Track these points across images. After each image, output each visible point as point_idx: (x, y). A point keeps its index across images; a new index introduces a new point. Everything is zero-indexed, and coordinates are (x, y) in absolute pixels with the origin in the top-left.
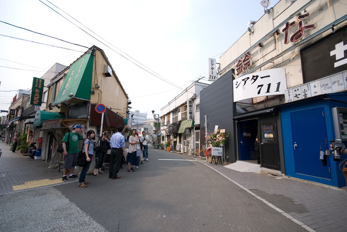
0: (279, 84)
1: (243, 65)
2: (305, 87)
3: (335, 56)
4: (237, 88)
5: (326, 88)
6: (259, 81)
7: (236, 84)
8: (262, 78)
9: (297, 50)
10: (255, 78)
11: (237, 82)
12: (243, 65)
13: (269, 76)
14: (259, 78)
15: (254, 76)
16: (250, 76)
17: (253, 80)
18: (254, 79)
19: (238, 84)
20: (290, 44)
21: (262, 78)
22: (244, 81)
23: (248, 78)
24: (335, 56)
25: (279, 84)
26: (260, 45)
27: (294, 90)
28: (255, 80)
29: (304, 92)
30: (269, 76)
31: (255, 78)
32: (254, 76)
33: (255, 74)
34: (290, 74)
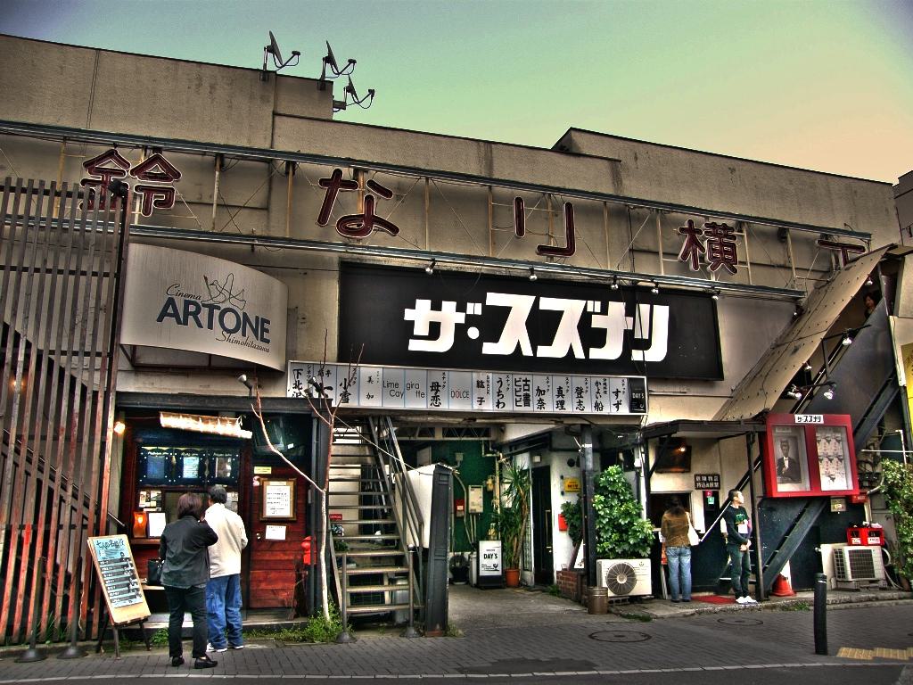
3: (412, 323)
5: (393, 393)
24: (412, 323)
29: (343, 385)
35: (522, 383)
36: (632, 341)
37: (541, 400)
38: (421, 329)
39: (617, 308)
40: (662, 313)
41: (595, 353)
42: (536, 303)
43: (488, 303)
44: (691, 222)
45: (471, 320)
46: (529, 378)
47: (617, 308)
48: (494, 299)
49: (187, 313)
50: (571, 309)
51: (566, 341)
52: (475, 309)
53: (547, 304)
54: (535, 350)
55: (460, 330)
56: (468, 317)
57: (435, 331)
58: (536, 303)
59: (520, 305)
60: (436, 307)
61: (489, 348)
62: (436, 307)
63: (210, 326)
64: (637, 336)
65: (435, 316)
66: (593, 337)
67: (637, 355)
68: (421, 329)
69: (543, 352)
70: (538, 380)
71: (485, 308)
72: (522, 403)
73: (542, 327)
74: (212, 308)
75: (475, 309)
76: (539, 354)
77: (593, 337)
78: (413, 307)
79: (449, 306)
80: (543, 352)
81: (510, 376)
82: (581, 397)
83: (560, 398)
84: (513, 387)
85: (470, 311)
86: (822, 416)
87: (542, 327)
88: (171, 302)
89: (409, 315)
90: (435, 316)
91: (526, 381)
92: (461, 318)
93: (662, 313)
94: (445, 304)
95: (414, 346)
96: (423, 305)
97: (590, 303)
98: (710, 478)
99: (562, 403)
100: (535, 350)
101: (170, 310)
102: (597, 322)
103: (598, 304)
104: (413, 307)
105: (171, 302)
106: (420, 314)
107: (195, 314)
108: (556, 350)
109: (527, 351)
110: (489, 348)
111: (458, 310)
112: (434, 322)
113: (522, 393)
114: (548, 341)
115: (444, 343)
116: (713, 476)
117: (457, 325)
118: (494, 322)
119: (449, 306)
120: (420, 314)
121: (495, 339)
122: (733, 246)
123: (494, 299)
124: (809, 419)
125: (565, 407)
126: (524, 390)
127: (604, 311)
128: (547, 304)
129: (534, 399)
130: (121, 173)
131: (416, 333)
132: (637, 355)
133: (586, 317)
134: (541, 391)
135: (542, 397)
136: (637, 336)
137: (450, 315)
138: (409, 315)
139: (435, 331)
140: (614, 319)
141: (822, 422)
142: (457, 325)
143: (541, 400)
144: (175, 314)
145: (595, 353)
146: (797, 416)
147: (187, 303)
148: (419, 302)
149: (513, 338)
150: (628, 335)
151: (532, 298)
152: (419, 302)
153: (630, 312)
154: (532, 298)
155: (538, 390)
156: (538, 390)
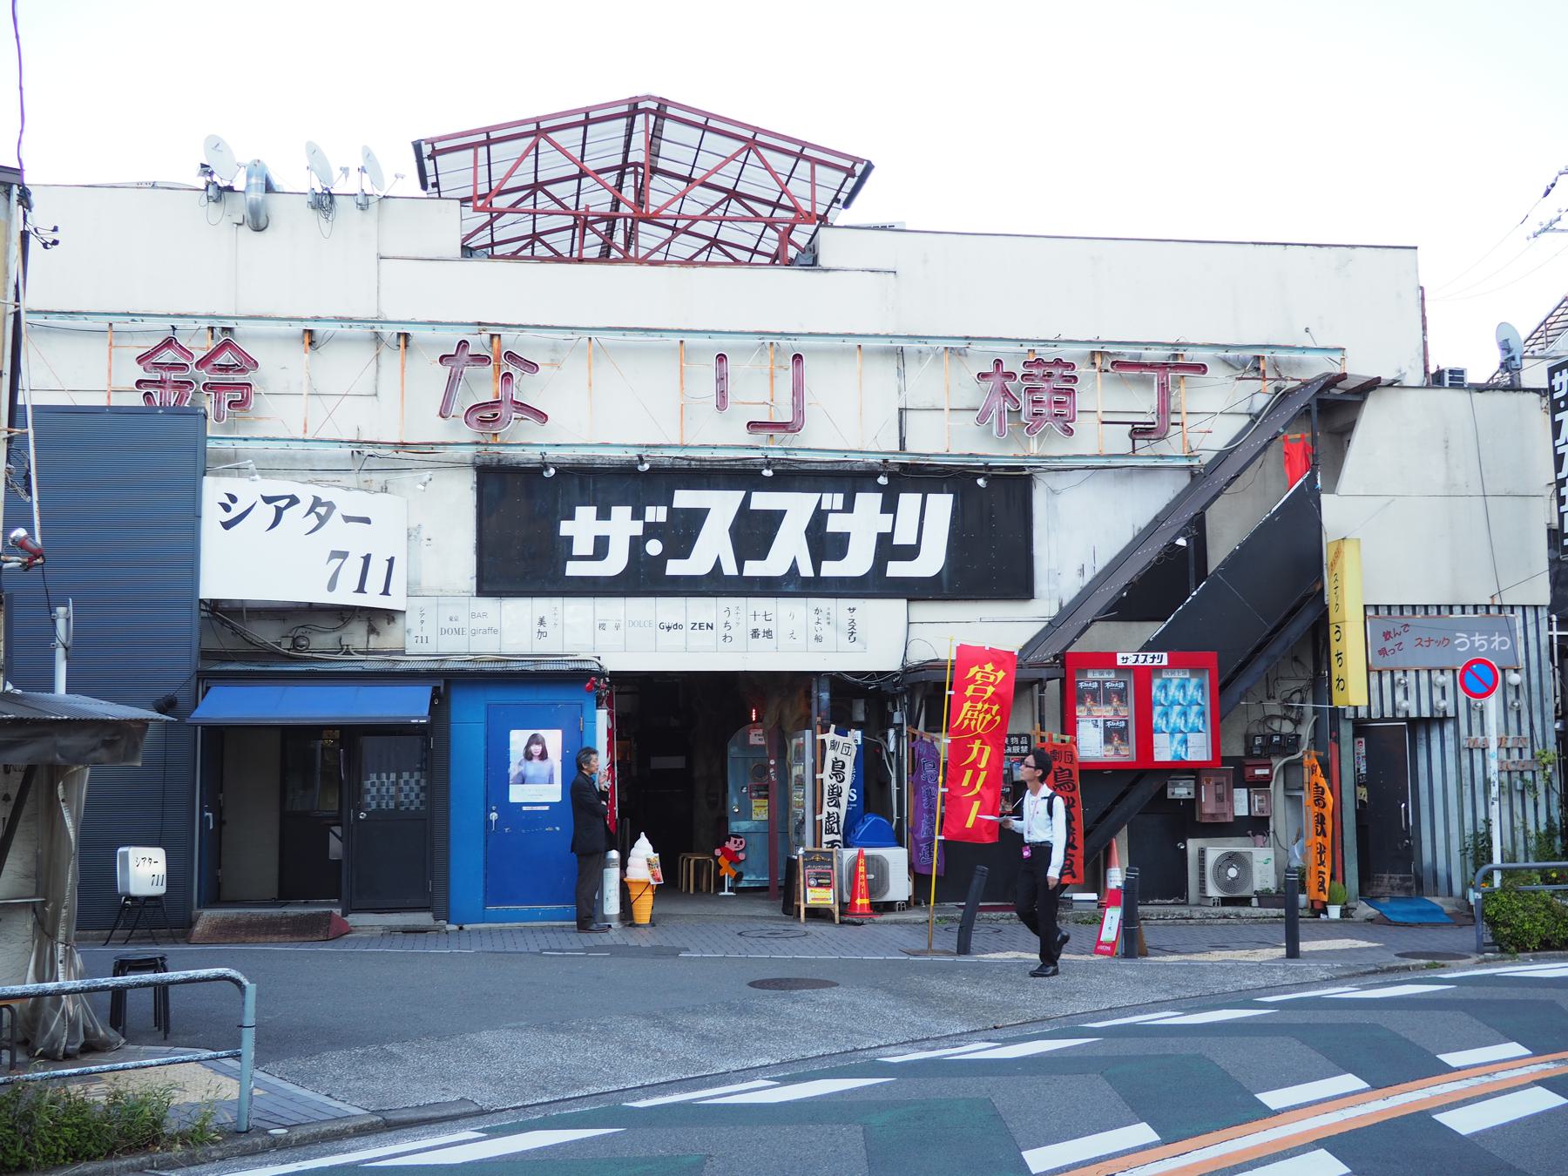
0: (391, 561)
3: (570, 540)
4: (227, 525)
6: (337, 533)
7: (227, 508)
8: (348, 519)
10: (321, 510)
11: (233, 499)
13: (367, 521)
14: (336, 517)
15: (317, 502)
16: (306, 494)
17: (313, 520)
18: (318, 514)
19: (237, 509)
20: (468, 434)
21: (348, 519)
22: (270, 510)
23: (294, 500)
24: (570, 540)
25: (391, 561)
28: (322, 520)
30: (367, 521)
31: (322, 510)
32: (317, 502)
33: (326, 495)
34: (424, 535)
36: (887, 548)
38: (583, 546)
39: (869, 502)
40: (941, 505)
41: (830, 569)
42: (746, 501)
44: (998, 363)
45: (652, 530)
47: (869, 502)
50: (797, 507)
51: (788, 550)
52: (656, 514)
53: (762, 501)
54: (740, 567)
55: (636, 544)
56: (647, 526)
57: (601, 547)
58: (746, 501)
59: (722, 506)
60: (604, 515)
61: (675, 568)
62: (604, 515)
64: (898, 540)
65: (603, 528)
66: (825, 543)
67: (896, 569)
68: (583, 546)
69: (753, 568)
71: (672, 512)
73: (754, 533)
75: (656, 514)
76: (745, 574)
77: (825, 543)
78: (571, 517)
79: (622, 513)
80: (753, 568)
86: (1165, 655)
87: (754, 533)
89: (566, 528)
90: (603, 528)
92: (637, 528)
93: (941, 505)
95: (573, 569)
96: (586, 513)
97: (827, 497)
98: (1014, 740)
100: (740, 567)
102: (835, 524)
103: (838, 500)
104: (571, 517)
106: (581, 527)
108: (773, 565)
109: (730, 568)
110: (675, 568)
112: (599, 534)
114: (762, 554)
115: (616, 562)
116: (1019, 736)
117: (633, 539)
118: (683, 531)
119: (622, 513)
120: (581, 527)
121: (685, 554)
122: (1070, 392)
123: (685, 499)
124: (1141, 659)
127: (848, 507)
128: (762, 501)
130: (183, 367)
132: (896, 569)
133: (820, 517)
136: (898, 540)
137: (622, 525)
138: (566, 528)
139: (601, 547)
140: (863, 521)
141: (1165, 662)
142: (633, 539)
145: (830, 569)
148: (579, 510)
149: (713, 548)
150: (884, 540)
151: (742, 494)
152: (579, 510)
153: (890, 507)
154: (739, 495)
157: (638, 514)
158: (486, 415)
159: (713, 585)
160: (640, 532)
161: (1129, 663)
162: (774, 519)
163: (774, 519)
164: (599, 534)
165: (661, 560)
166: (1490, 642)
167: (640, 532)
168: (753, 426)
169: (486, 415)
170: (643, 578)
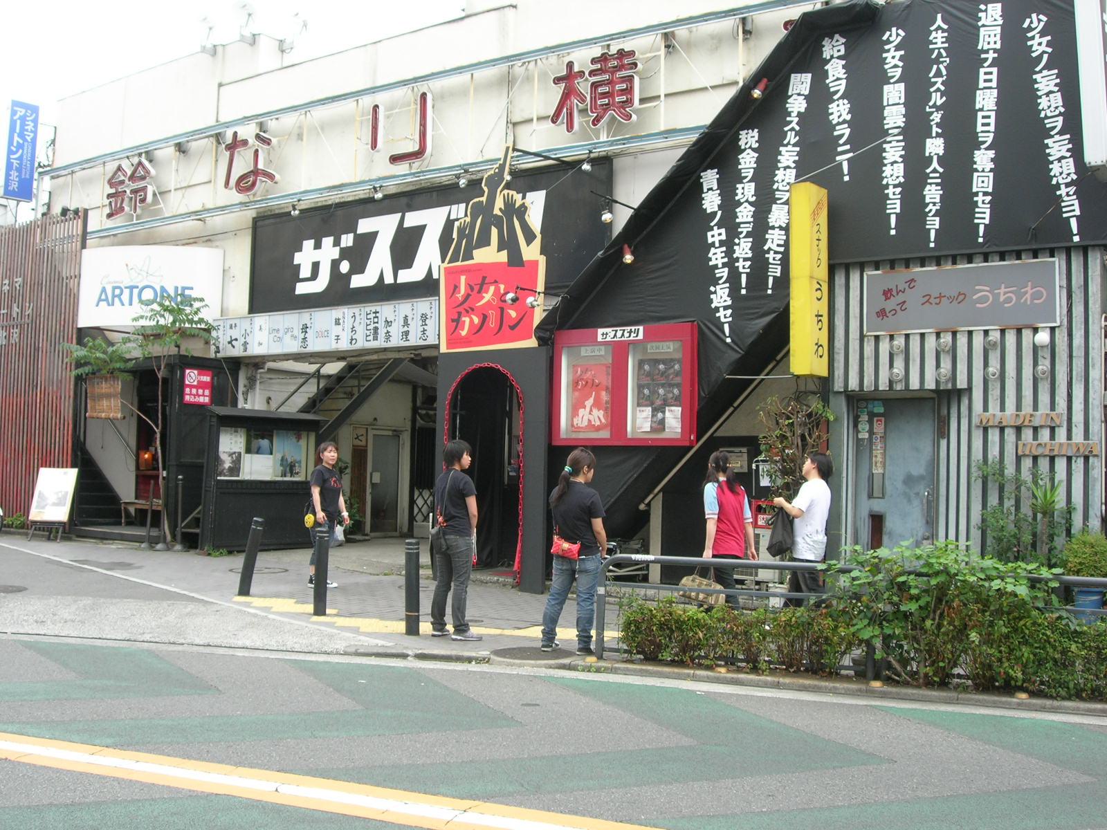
1: (128, 192)
2: (245, 325)
9: (251, 214)
12: (128, 192)
20: (235, 197)
26: (181, 148)
27: (230, 322)
35: (372, 316)
37: (388, 332)
38: (305, 272)
43: (360, 231)
46: (378, 309)
48: (365, 226)
49: (114, 296)
52: (347, 240)
55: (335, 264)
56: (342, 250)
59: (384, 227)
60: (318, 246)
62: (318, 246)
63: (131, 304)
69: (405, 276)
70: (387, 310)
72: (371, 338)
74: (131, 288)
75: (347, 240)
81: (362, 309)
82: (426, 325)
83: (406, 329)
84: (365, 321)
85: (343, 245)
86: (641, 328)
88: (104, 290)
91: (376, 312)
92: (335, 253)
94: (324, 240)
95: (302, 289)
97: (454, 207)
99: (407, 333)
101: (103, 297)
105: (104, 290)
107: (119, 296)
109: (389, 279)
110: (357, 281)
111: (335, 245)
113: (371, 327)
118: (359, 254)
119: (328, 241)
123: (365, 226)
125: (409, 337)
126: (374, 323)
128: (413, 219)
129: (382, 332)
131: (301, 276)
134: (388, 322)
135: (388, 329)
137: (328, 251)
143: (388, 332)
144: (106, 299)
146: (600, 331)
147: (114, 288)
149: (380, 263)
151: (399, 215)
154: (398, 216)
155: (386, 321)
156: (386, 321)
157: (337, 243)
158: (246, 183)
159: (383, 292)
160: (337, 256)
161: (608, 339)
162: (419, 230)
163: (419, 230)
164: (316, 259)
165: (347, 277)
166: (1020, 295)
167: (337, 256)
168: (395, 159)
169: (246, 183)
170: (340, 293)
